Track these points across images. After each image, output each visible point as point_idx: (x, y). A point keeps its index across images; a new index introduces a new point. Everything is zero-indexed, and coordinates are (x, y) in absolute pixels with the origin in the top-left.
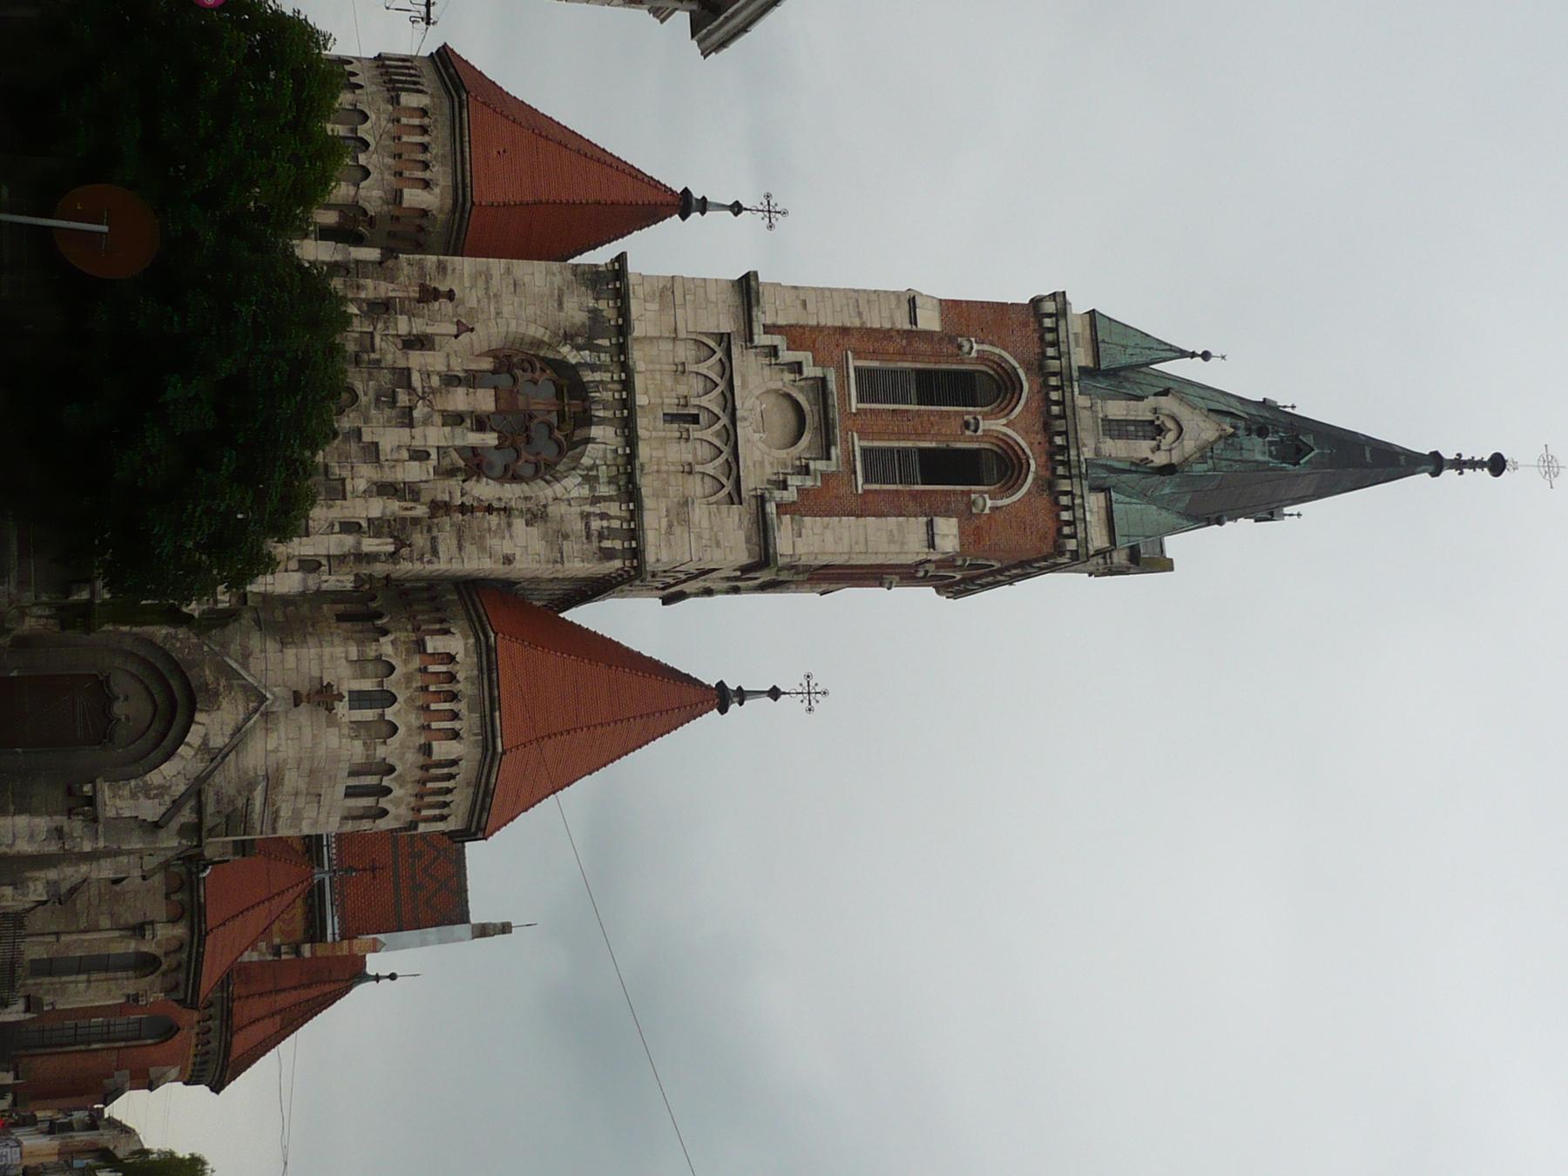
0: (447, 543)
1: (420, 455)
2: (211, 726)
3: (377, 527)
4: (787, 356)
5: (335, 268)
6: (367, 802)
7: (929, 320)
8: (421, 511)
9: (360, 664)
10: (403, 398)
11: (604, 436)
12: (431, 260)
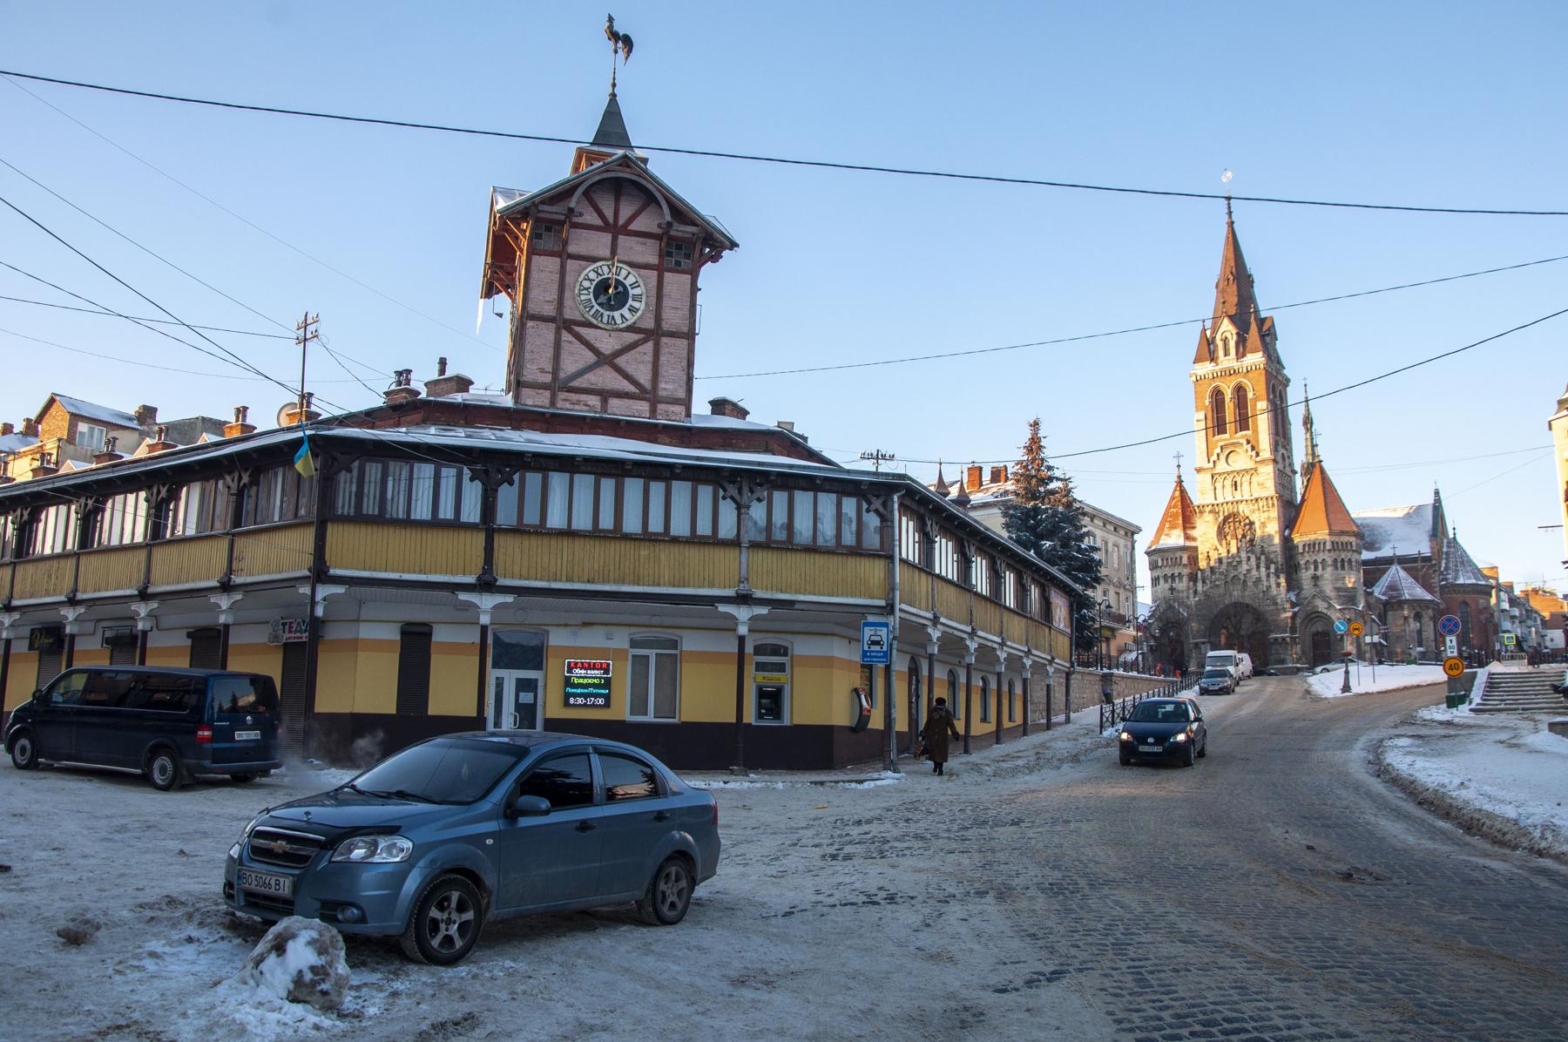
0: (1272, 549)
1: (1249, 559)
2: (1321, 606)
3: (1268, 568)
4: (1214, 458)
5: (1204, 582)
6: (1346, 564)
7: (1201, 415)
8: (1263, 558)
9: (1307, 569)
10: (1235, 563)
11: (1242, 508)
12: (1200, 557)
